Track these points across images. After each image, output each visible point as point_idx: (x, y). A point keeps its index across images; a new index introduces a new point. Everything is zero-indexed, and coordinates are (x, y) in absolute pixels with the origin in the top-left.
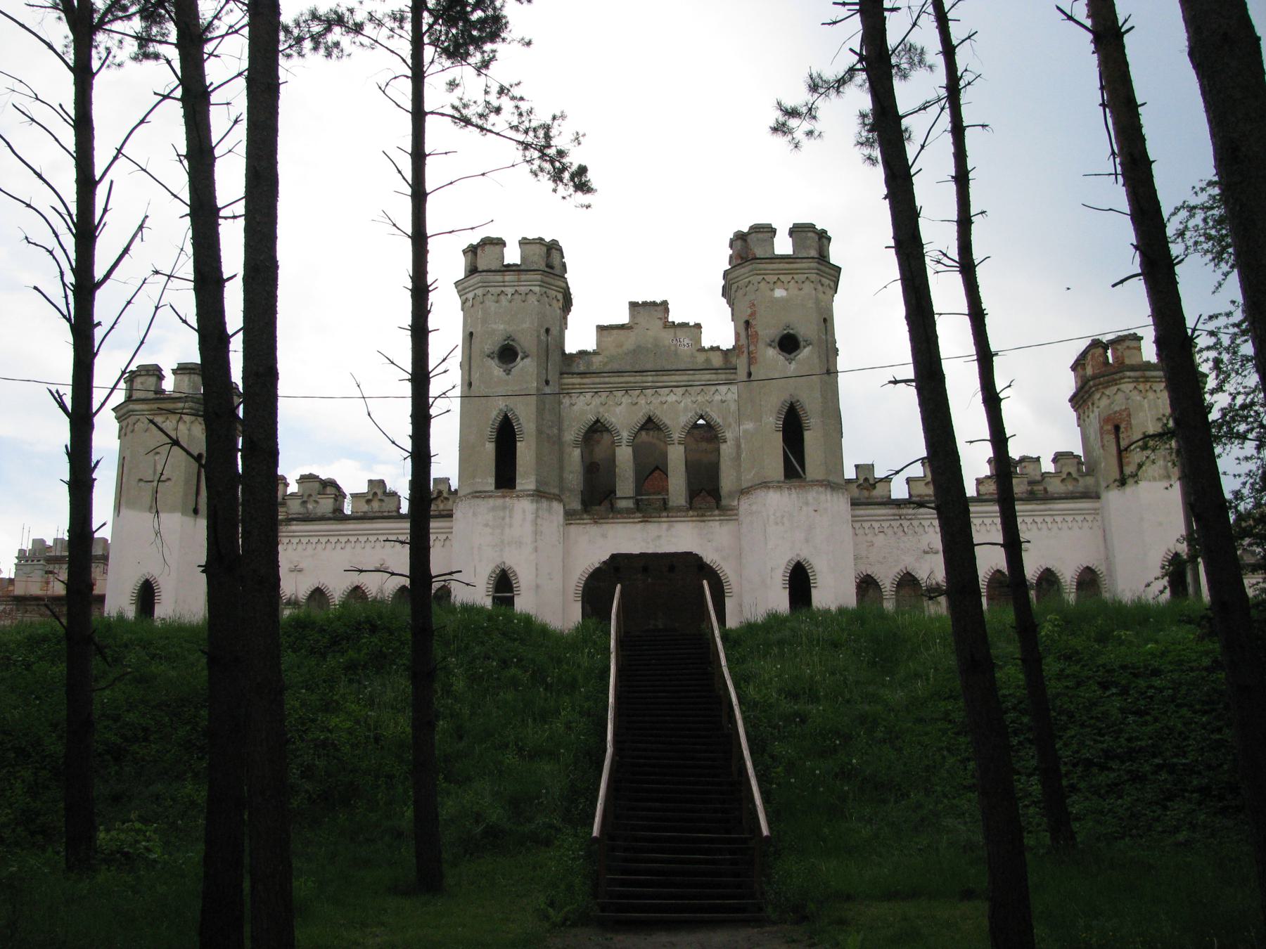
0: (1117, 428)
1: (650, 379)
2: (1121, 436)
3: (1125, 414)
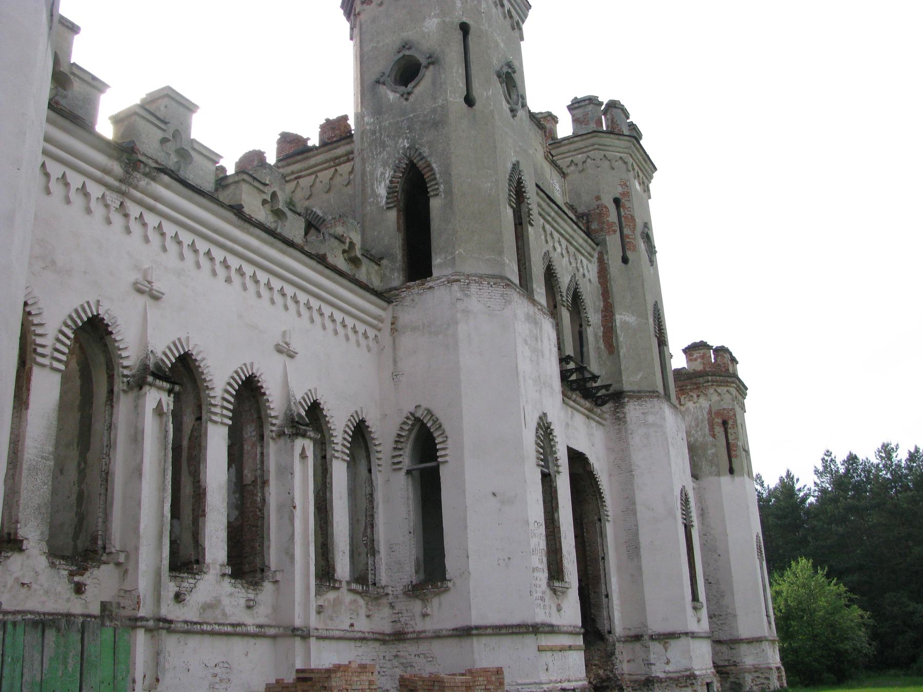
0: (725, 423)
1: (553, 214)
2: (729, 431)
3: (731, 413)
